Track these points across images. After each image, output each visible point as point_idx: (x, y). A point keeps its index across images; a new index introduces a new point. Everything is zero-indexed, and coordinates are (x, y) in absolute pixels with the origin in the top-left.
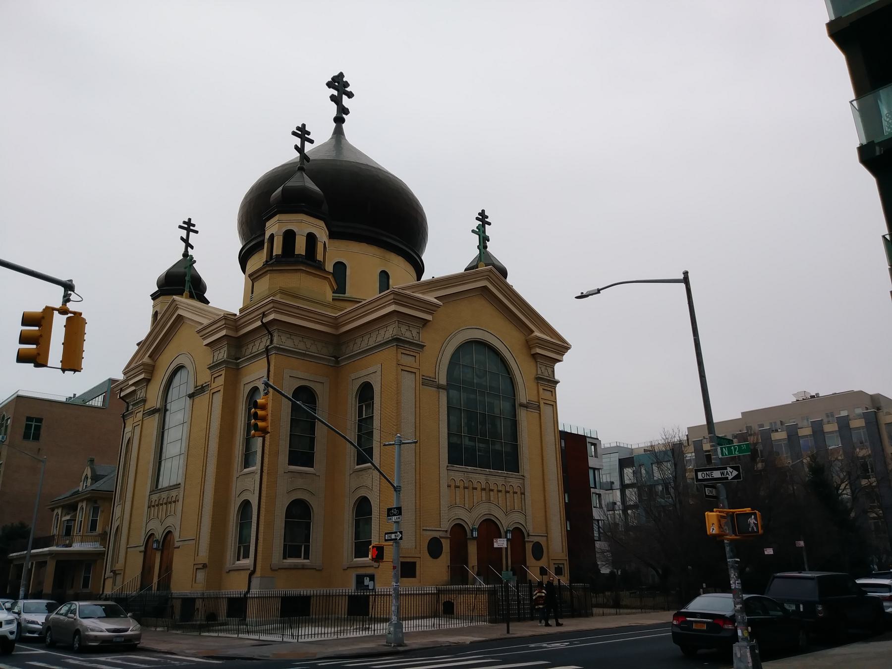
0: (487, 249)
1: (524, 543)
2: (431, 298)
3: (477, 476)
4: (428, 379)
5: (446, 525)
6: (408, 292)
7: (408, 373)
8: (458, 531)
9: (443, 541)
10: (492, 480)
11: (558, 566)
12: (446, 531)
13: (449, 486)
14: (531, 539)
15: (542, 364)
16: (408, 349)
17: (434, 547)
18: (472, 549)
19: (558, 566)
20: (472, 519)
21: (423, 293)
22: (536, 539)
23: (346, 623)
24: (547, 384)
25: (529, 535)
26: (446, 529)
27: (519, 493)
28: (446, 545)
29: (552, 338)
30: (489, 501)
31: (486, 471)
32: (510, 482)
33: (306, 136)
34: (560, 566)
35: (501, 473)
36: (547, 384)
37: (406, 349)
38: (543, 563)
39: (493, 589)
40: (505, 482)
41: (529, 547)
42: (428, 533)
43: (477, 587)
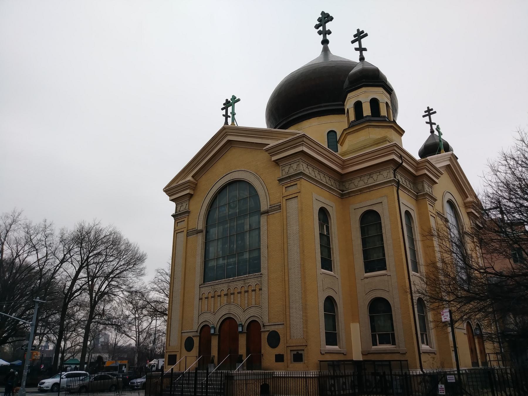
0: (365, 60)
1: (259, 334)
2: (189, 178)
3: (206, 288)
4: (192, 230)
5: (196, 327)
6: (172, 186)
7: (180, 233)
8: (205, 329)
9: (194, 339)
10: (219, 288)
11: (297, 353)
12: (197, 331)
13: (201, 299)
14: (268, 329)
15: (286, 165)
16: (180, 218)
17: (189, 344)
18: (215, 342)
19: (297, 353)
20: (214, 320)
21: (184, 178)
22: (272, 328)
23: (126, 392)
24: (289, 180)
25: (264, 326)
26: (196, 330)
27: (257, 290)
28: (196, 341)
29: (280, 139)
30: (229, 303)
31: (244, 277)
32: (248, 283)
33: (235, 100)
34: (300, 352)
35: (246, 276)
36: (289, 180)
37: (179, 219)
38: (278, 350)
39: (150, 375)
40: (245, 284)
41: (264, 337)
42: (186, 334)
43: (158, 373)
